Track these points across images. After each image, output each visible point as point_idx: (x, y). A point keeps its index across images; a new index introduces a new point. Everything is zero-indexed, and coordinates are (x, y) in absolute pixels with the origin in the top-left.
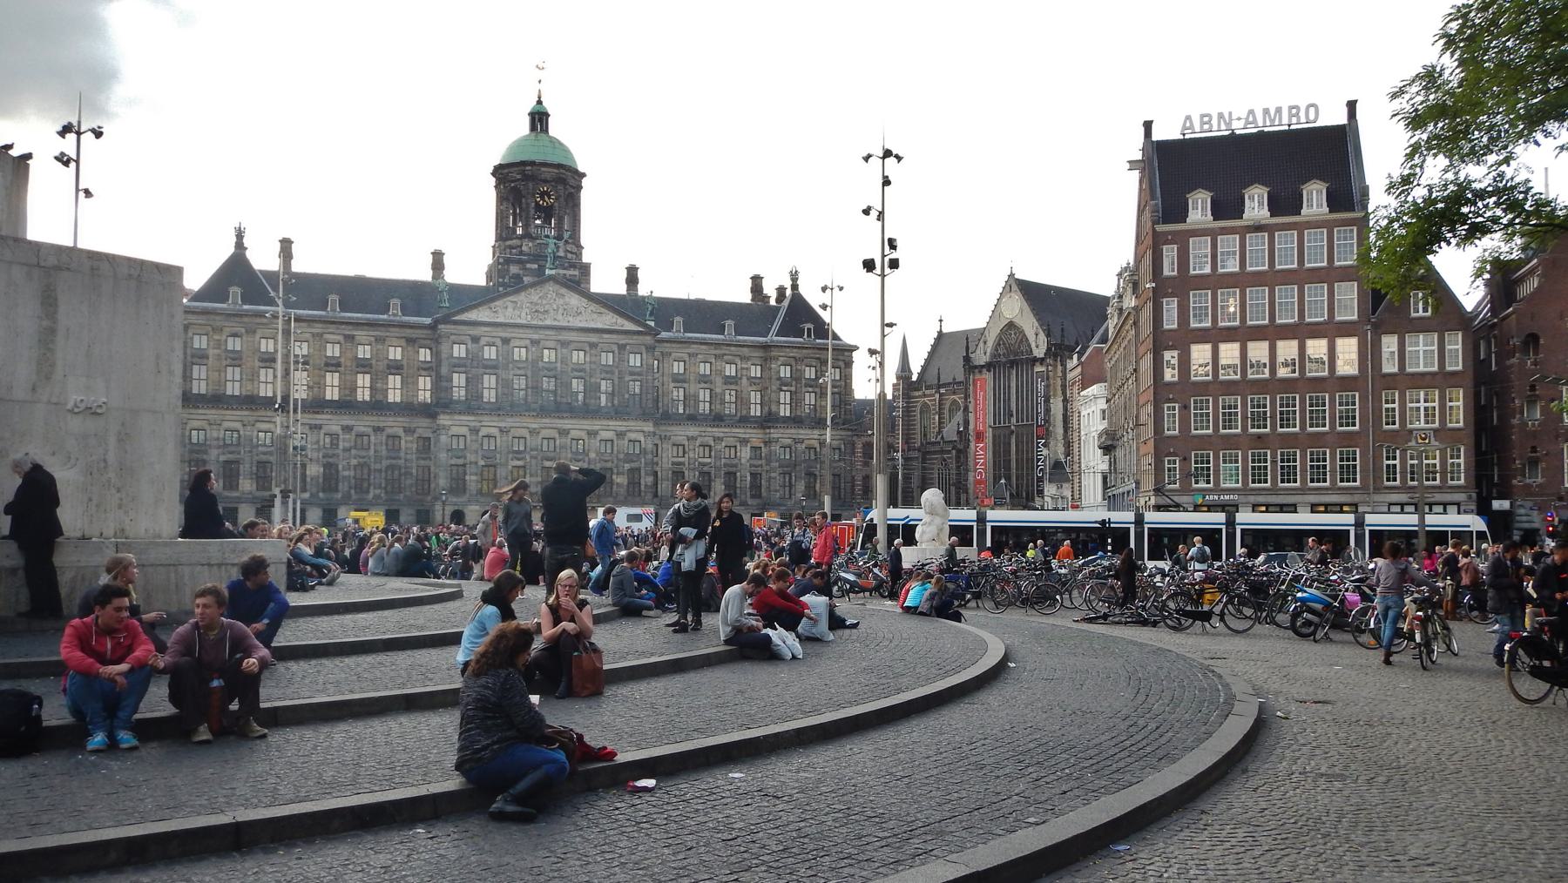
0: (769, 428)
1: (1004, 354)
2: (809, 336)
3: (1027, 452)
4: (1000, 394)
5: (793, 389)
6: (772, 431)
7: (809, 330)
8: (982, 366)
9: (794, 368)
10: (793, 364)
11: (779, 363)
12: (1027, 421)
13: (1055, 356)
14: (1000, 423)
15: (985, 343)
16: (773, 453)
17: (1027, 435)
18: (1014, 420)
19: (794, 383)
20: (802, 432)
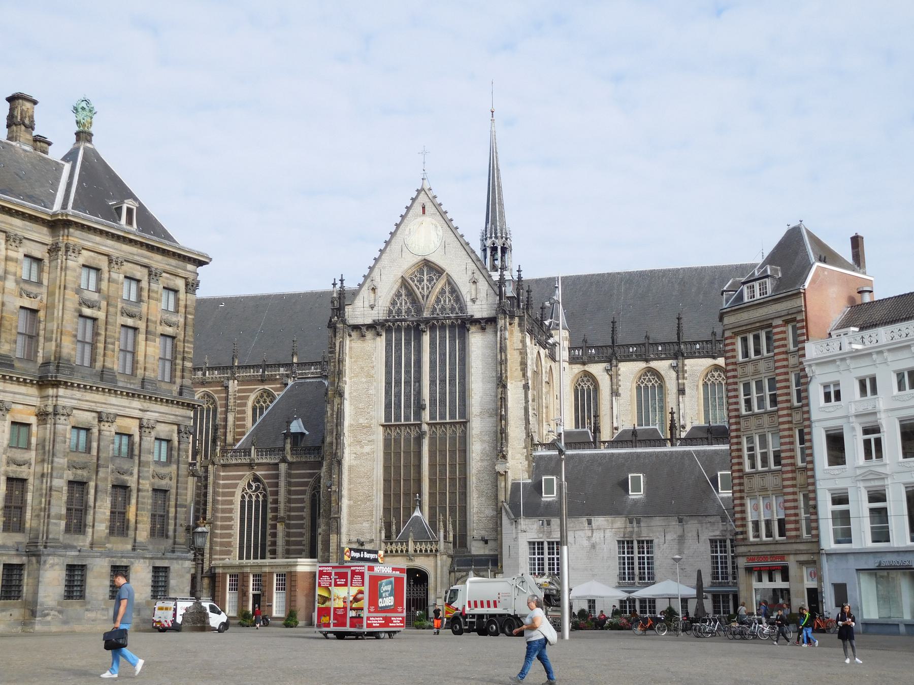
0: (56, 384)
1: (408, 311)
2: (129, 222)
3: (453, 466)
4: (398, 372)
5: (101, 315)
6: (61, 391)
7: (130, 211)
8: (370, 327)
9: (106, 275)
10: (103, 263)
11: (81, 260)
12: (452, 416)
13: (512, 317)
14: (398, 418)
15: (374, 289)
16: (59, 439)
17: (453, 439)
18: (426, 415)
19: (104, 304)
20: (113, 400)
